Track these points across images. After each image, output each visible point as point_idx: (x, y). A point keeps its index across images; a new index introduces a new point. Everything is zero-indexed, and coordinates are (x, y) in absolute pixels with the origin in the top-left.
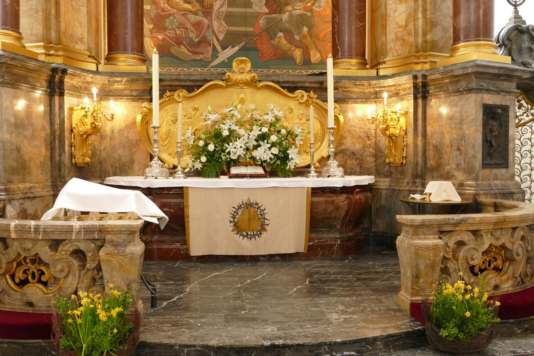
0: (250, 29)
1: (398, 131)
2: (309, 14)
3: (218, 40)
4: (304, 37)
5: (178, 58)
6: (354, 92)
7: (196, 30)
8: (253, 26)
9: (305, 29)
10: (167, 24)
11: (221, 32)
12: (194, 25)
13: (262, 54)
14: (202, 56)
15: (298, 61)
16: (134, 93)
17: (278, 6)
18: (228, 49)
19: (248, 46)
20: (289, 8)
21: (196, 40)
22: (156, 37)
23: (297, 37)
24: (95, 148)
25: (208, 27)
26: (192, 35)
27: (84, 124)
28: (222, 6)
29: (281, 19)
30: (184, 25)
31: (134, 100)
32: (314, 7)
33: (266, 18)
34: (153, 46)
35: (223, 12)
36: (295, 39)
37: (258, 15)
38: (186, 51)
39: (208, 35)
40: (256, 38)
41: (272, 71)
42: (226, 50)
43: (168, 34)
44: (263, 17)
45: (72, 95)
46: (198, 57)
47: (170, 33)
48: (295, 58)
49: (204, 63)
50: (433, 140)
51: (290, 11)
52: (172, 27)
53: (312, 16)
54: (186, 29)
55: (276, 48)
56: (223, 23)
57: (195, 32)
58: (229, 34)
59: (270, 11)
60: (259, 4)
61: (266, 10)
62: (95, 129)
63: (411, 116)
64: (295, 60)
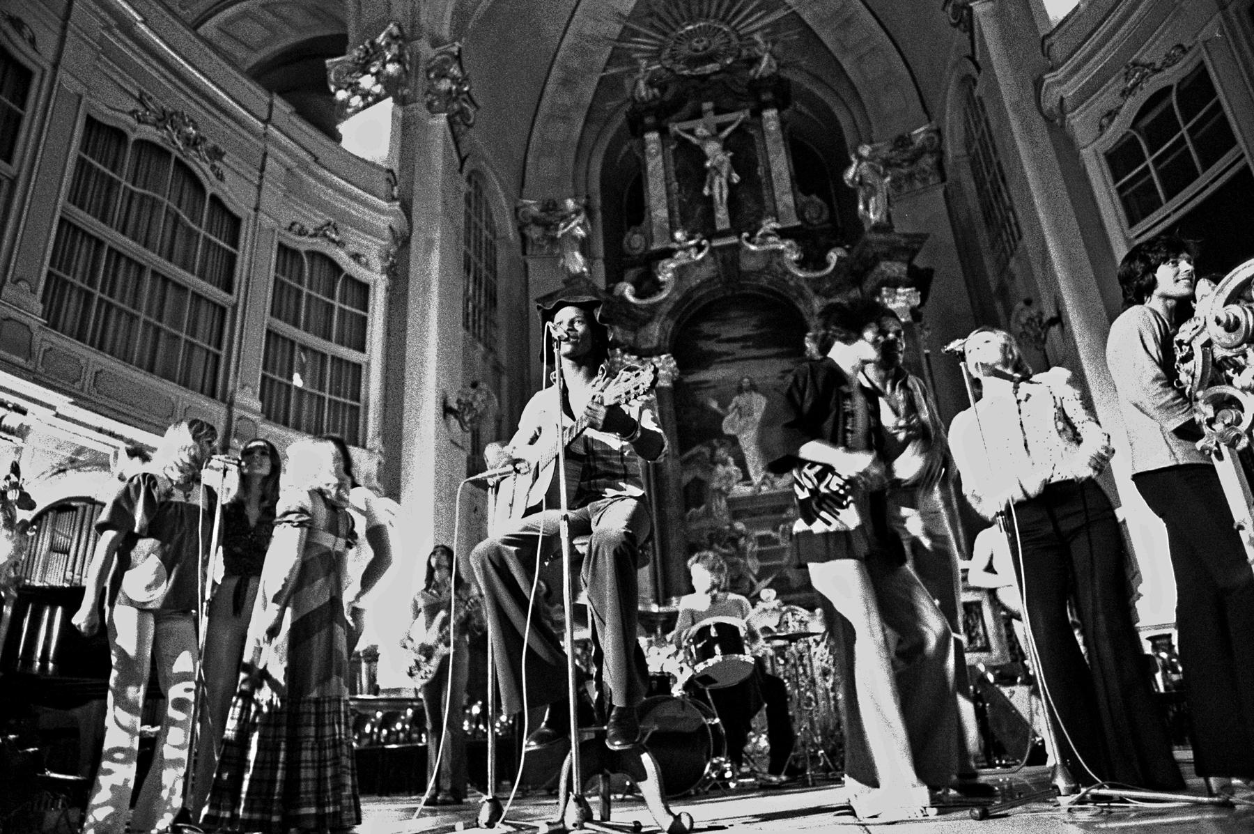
3: (753, 575)
37: (784, 549)
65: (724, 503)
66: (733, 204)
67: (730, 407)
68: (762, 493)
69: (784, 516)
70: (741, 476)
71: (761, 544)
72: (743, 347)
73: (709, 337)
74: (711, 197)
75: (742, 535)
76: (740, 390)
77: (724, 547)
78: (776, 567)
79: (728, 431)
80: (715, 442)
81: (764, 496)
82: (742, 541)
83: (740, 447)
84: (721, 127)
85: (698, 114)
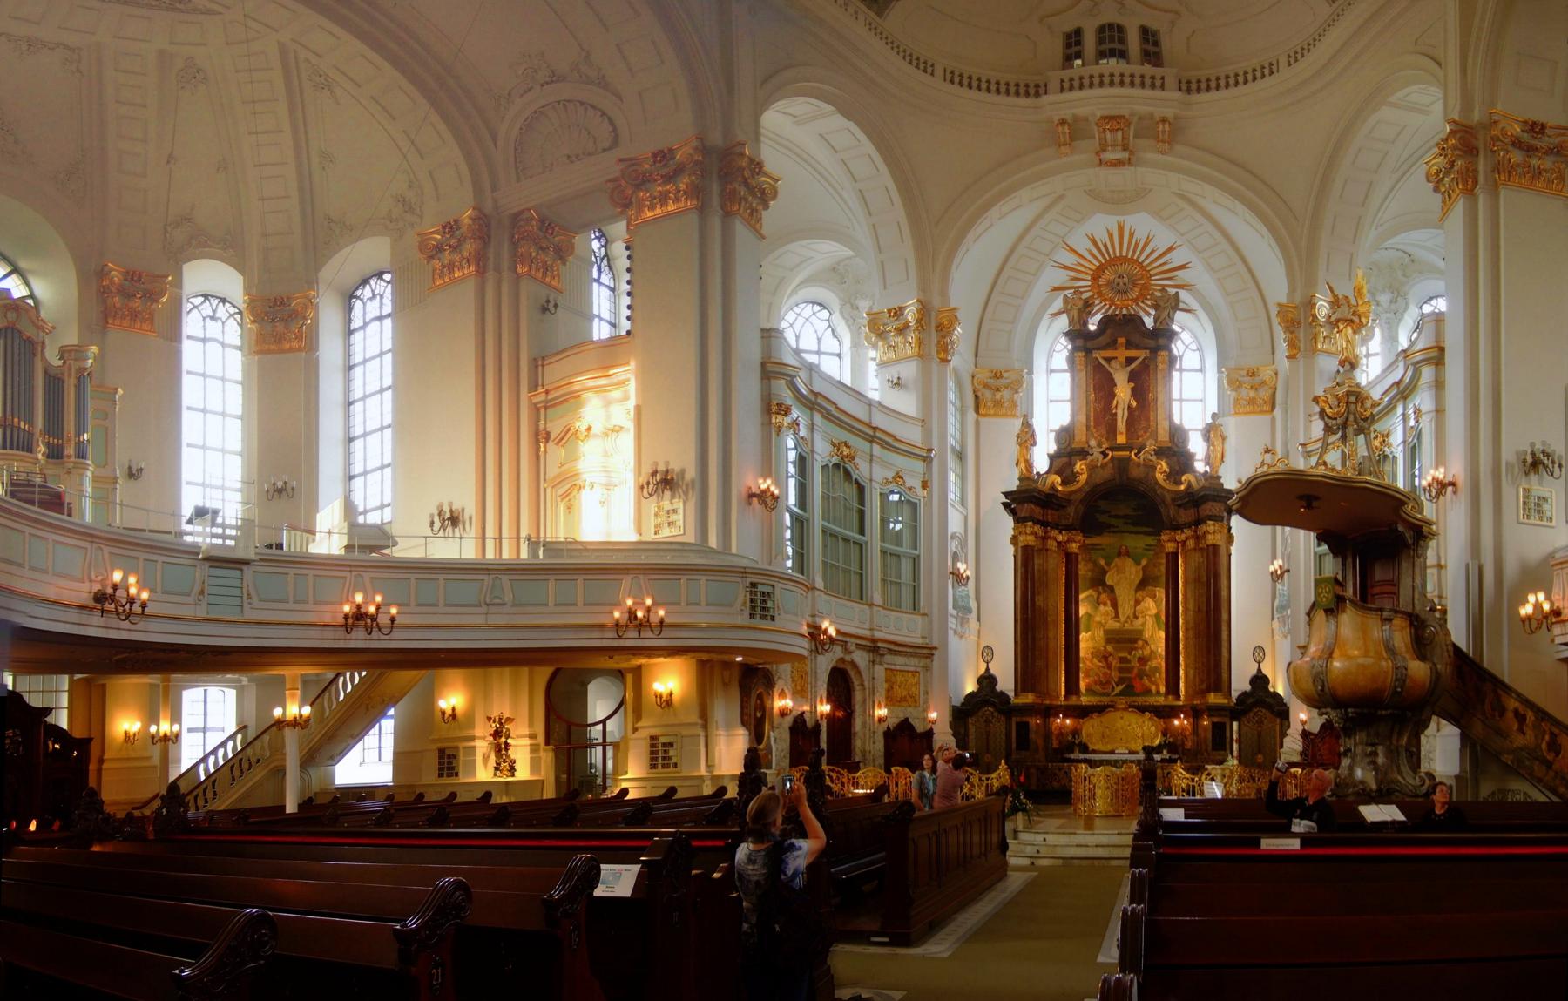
66: (1131, 423)
67: (1113, 565)
72: (1126, 523)
74: (1116, 414)
76: (1119, 554)
79: (1109, 581)
81: (1127, 631)
84: (1129, 361)
85: (1112, 344)
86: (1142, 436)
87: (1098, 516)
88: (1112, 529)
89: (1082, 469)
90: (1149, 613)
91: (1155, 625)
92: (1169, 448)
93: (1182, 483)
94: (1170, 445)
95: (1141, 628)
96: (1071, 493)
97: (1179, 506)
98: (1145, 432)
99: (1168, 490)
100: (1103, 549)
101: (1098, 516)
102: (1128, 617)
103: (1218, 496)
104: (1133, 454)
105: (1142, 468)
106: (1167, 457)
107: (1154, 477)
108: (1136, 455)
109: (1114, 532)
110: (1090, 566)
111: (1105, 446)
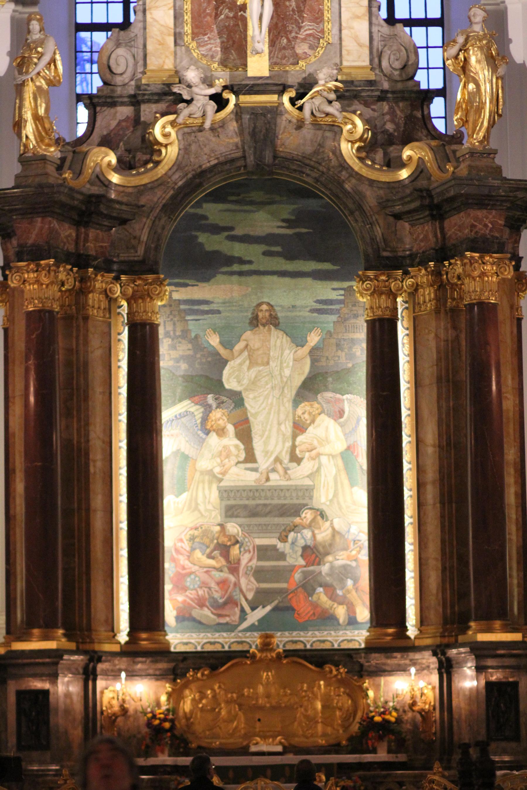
0: (284, 585)
1: (427, 707)
2: (354, 564)
3: (246, 599)
4: (349, 592)
5: (200, 623)
6: (388, 665)
7: (221, 589)
8: (287, 582)
9: (350, 583)
10: (188, 584)
11: (249, 590)
12: (218, 584)
13: (298, 614)
14: (227, 619)
15: (341, 621)
16: (158, 673)
17: (317, 556)
18: (259, 609)
19: (281, 605)
20: (330, 558)
21: (221, 601)
22: (176, 599)
23: (340, 592)
24: (119, 729)
25: (235, 584)
26: (216, 595)
27: (112, 706)
28: (250, 560)
29: (320, 573)
30: (207, 584)
31: (157, 680)
32: (359, 556)
33: (303, 572)
34: (171, 608)
35: (251, 566)
36: (337, 595)
37: (292, 569)
38: (209, 613)
39: (234, 594)
40: (291, 595)
41: (310, 633)
42: (256, 611)
43: (190, 595)
44: (300, 571)
45: (102, 679)
46: (223, 621)
47: (191, 594)
48: (338, 617)
49: (230, 628)
50: (456, 716)
51: (331, 563)
52: (194, 586)
53: (357, 566)
54: (210, 588)
55: (315, 606)
56: (252, 579)
57: (220, 591)
58: (259, 592)
59: (307, 563)
60: (294, 556)
61: (302, 562)
62: (124, 711)
63: (437, 691)
64: (337, 620)
65: (214, 495)
68: (268, 484)
69: (297, 520)
70: (243, 456)
71: (259, 559)
72: (265, 254)
73: (216, 229)
75: (237, 542)
77: (210, 556)
78: (281, 591)
80: (210, 399)
82: (235, 551)
83: (246, 409)
86: (306, 56)
87: (203, 238)
88: (236, 267)
89: (166, 135)
90: (327, 449)
91: (343, 476)
92: (371, 83)
93: (403, 165)
94: (372, 77)
95: (308, 482)
96: (142, 190)
97: (398, 217)
98: (313, 47)
99: (372, 182)
100: (219, 312)
101: (203, 238)
102: (278, 460)
103: (489, 197)
104: (286, 99)
105: (308, 132)
106: (366, 104)
107: (337, 153)
108: (292, 101)
109: (241, 274)
110: (185, 348)
111: (219, 83)
